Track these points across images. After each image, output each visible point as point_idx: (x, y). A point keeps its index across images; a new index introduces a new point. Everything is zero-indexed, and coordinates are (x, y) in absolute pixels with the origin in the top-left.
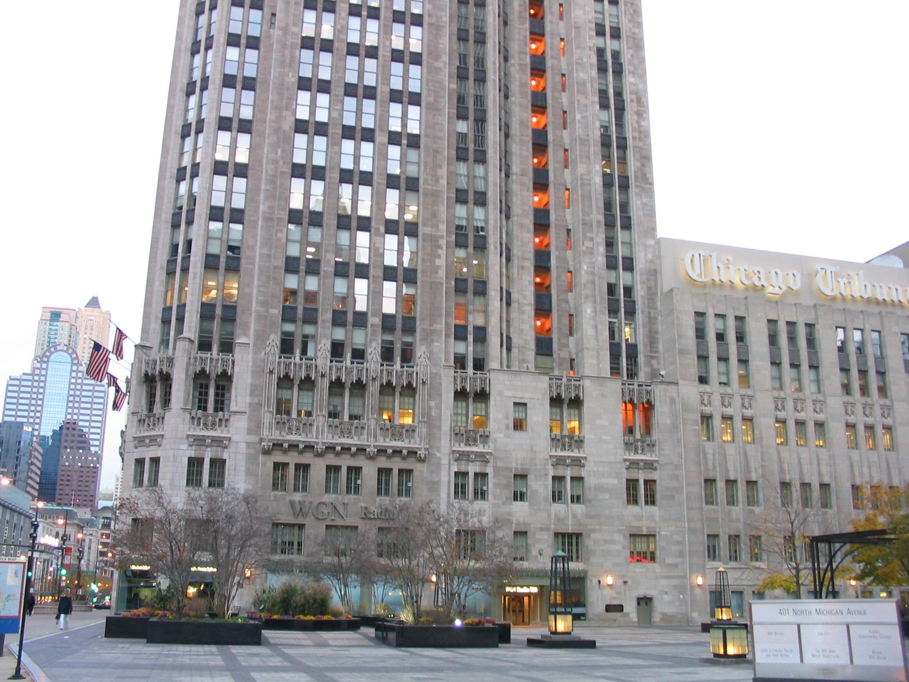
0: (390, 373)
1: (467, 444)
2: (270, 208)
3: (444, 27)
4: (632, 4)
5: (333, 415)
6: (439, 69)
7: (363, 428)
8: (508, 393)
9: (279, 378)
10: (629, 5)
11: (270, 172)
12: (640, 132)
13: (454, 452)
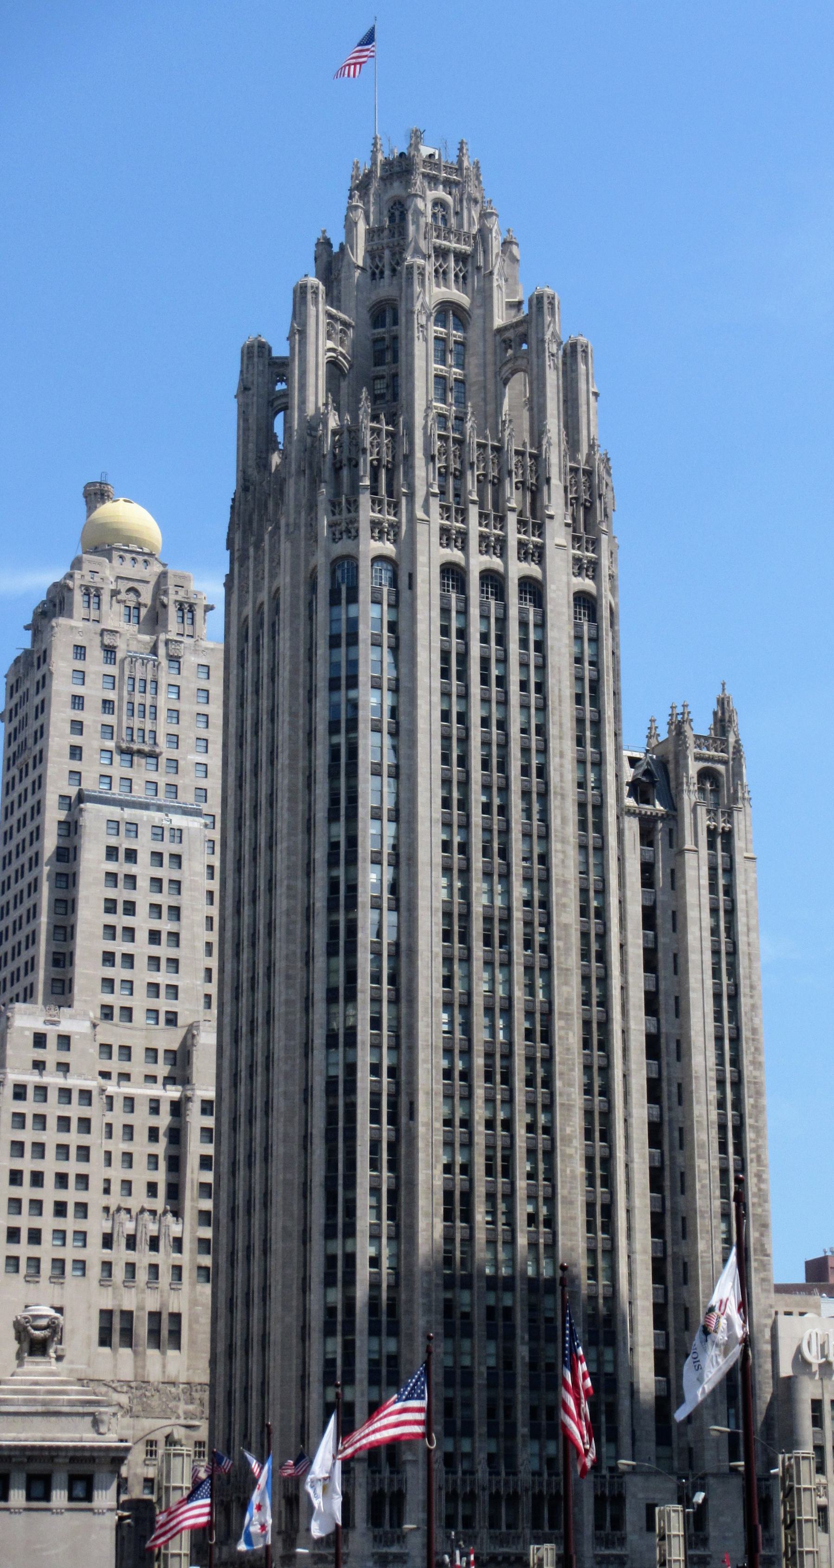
0: (541, 1484)
1: (607, 1547)
2: (428, 1322)
3: (573, 1106)
4: (753, 1040)
5: (494, 1523)
6: (571, 1156)
7: (519, 1537)
8: (641, 1495)
9: (447, 1494)
10: (750, 1042)
11: (425, 1285)
12: (760, 1197)
13: (596, 1556)
